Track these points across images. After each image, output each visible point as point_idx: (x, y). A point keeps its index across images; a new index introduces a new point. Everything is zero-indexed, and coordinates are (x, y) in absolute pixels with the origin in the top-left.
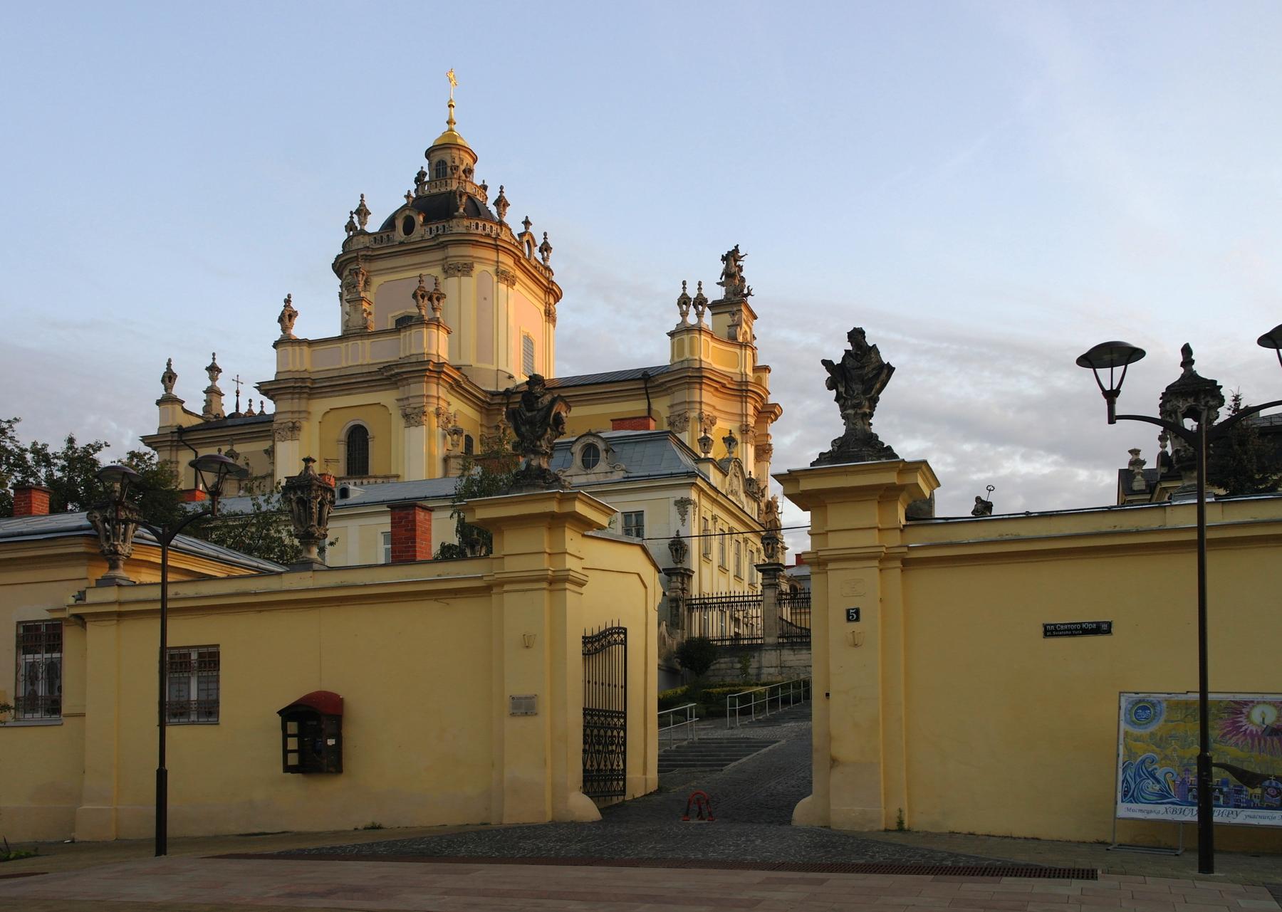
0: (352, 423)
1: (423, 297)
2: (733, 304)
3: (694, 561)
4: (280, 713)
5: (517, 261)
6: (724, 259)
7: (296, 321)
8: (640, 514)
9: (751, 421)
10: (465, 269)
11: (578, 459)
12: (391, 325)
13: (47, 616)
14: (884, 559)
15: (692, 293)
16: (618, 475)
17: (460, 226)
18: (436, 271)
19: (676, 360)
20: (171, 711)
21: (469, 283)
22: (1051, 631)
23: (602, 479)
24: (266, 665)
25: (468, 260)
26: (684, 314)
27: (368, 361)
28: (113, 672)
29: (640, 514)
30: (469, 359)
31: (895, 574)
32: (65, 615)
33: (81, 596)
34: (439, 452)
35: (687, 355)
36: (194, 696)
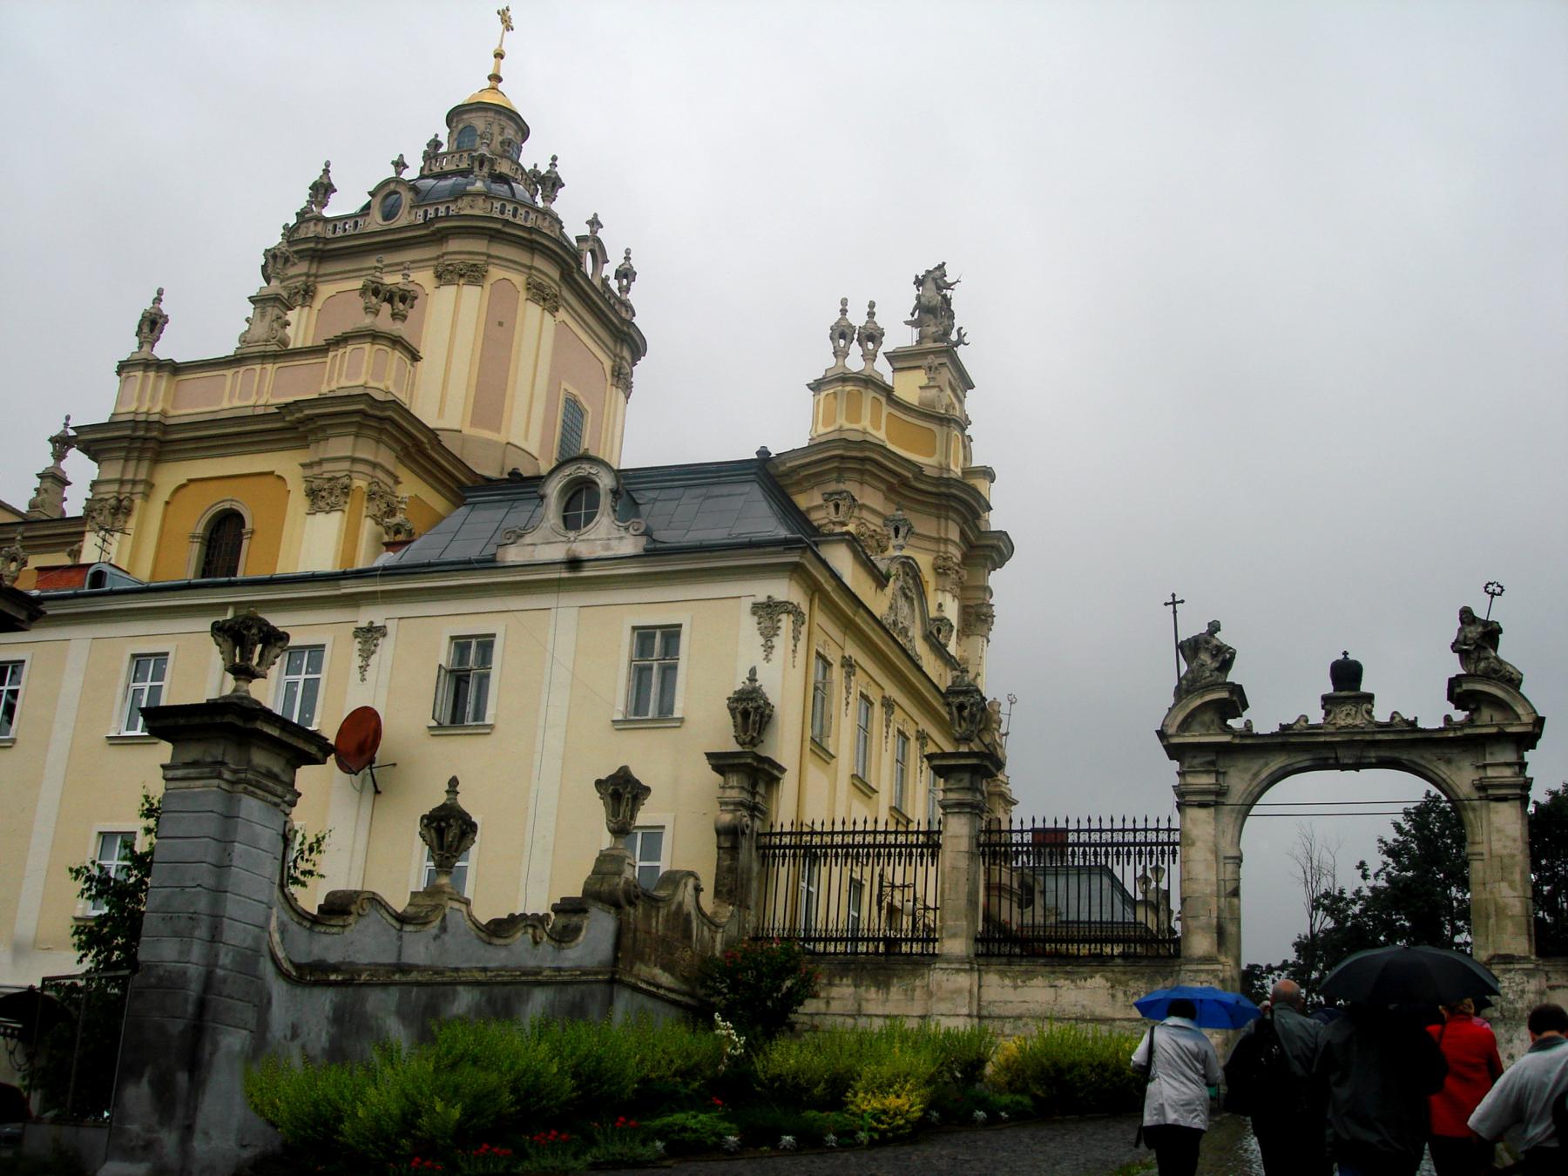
0: (227, 505)
3: (785, 745)
6: (919, 282)
8: (672, 634)
9: (955, 553)
10: (473, 274)
11: (552, 510)
15: (857, 319)
18: (424, 278)
19: (821, 430)
21: (472, 297)
29: (672, 634)
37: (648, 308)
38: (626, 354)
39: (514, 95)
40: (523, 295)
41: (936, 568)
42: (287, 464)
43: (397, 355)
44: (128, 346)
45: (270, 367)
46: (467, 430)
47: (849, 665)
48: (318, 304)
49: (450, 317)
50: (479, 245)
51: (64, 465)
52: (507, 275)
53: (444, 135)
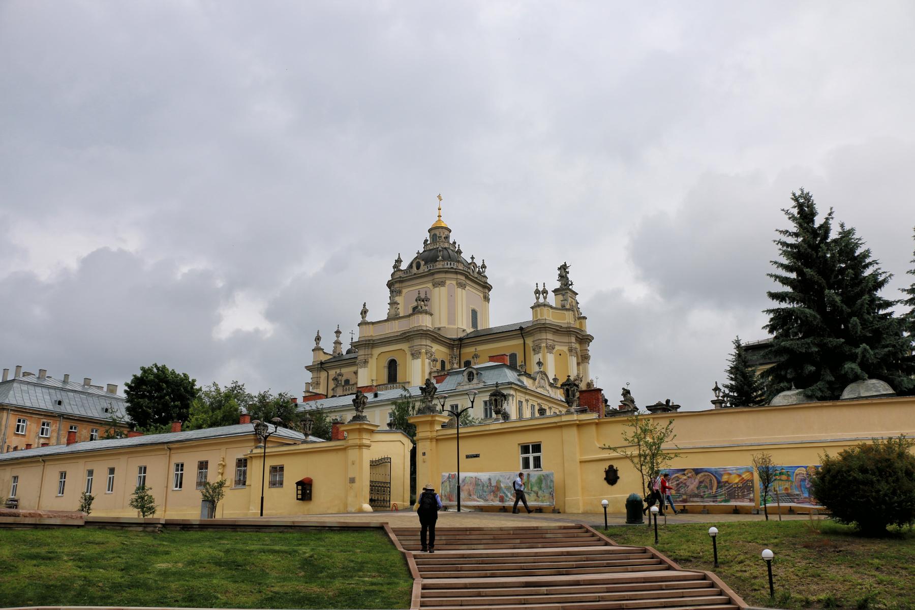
2: (564, 290)
5: (467, 277)
6: (559, 269)
7: (368, 314)
10: (442, 284)
12: (410, 311)
15: (541, 289)
16: (481, 385)
18: (430, 285)
22: (477, 456)
23: (476, 387)
26: (538, 298)
30: (443, 323)
31: (434, 443)
34: (427, 371)
35: (539, 317)
37: (491, 276)
39: (446, 223)
42: (404, 346)
43: (428, 316)
44: (360, 320)
47: (527, 401)
48: (403, 294)
49: (440, 296)
50: (443, 275)
51: (340, 339)
52: (451, 283)
53: (428, 236)
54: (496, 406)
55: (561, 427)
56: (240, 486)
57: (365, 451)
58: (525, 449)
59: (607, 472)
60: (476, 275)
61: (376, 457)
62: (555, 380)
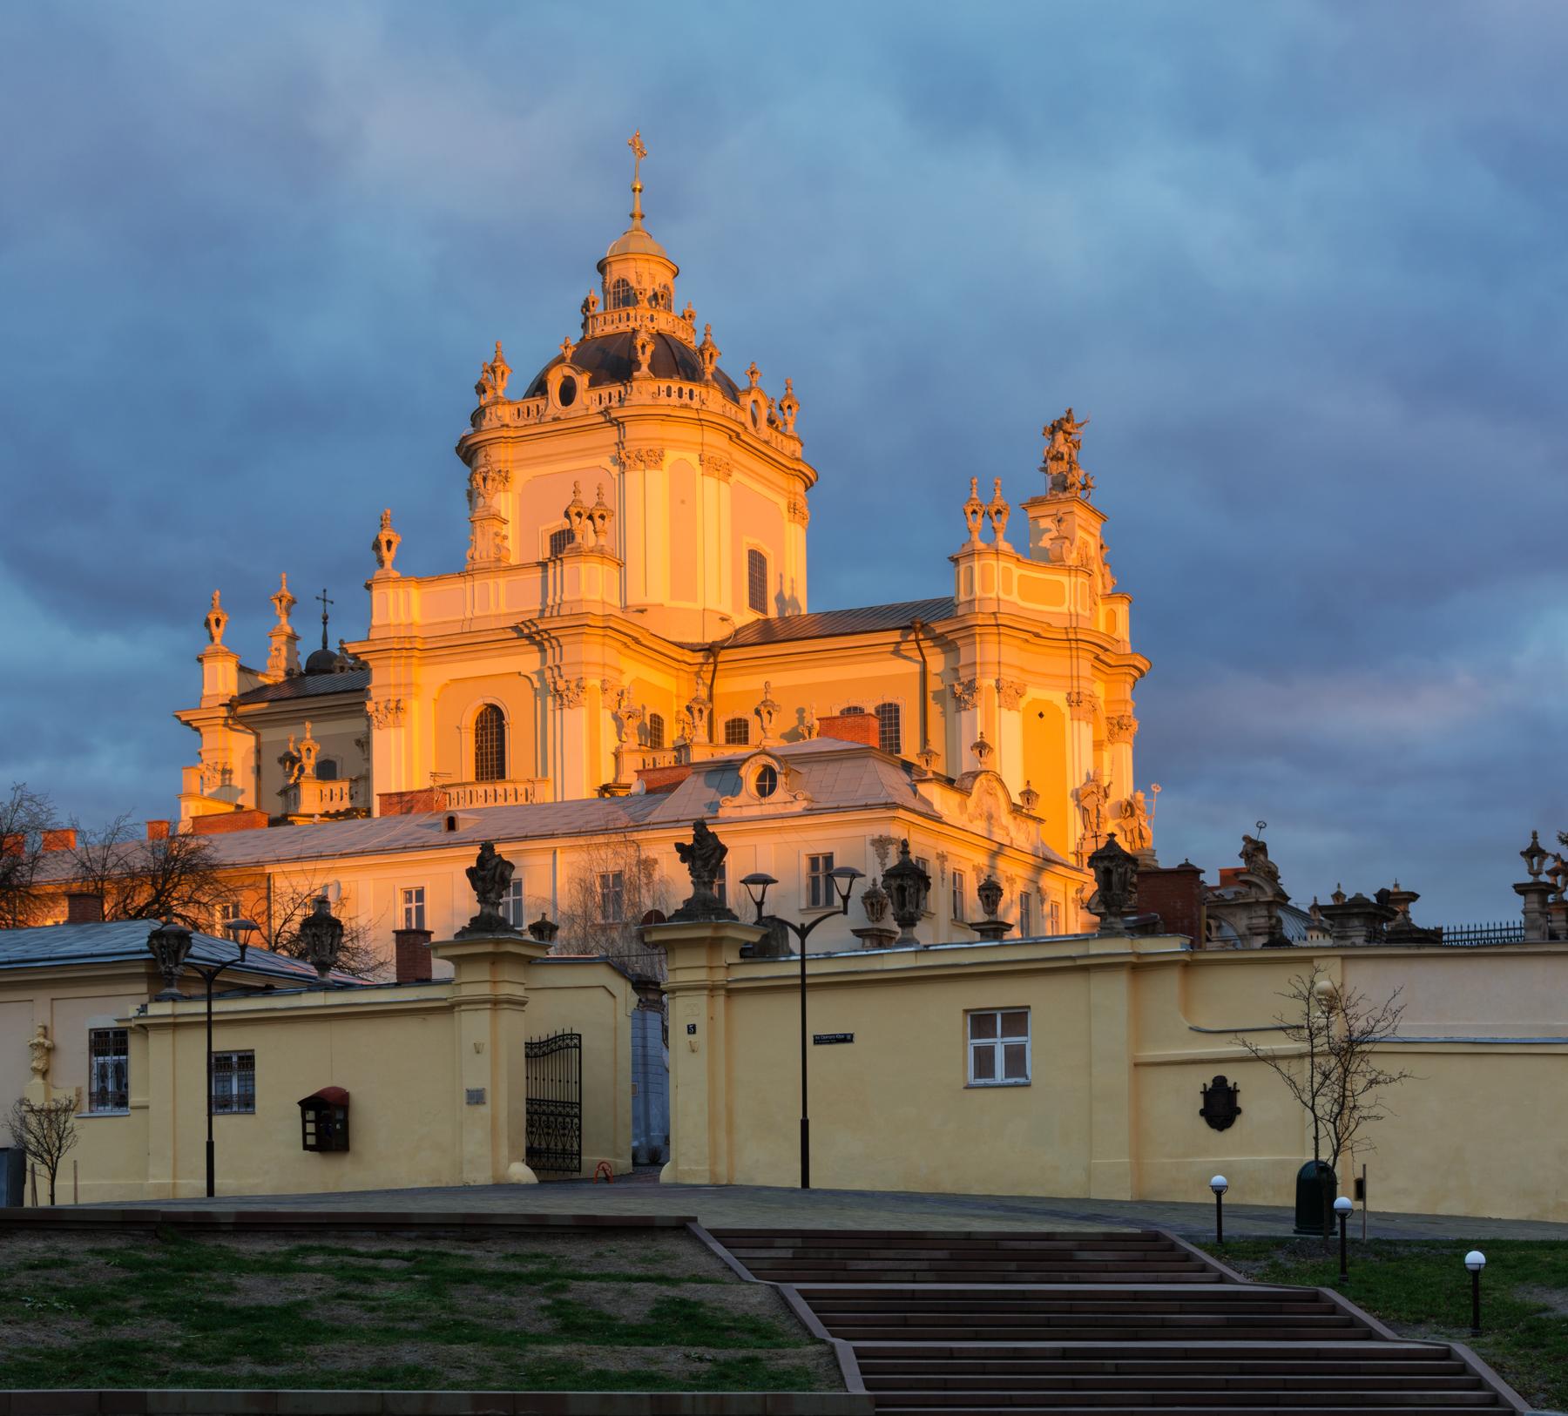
1: (579, 515)
4: (300, 1103)
5: (735, 437)
10: (653, 459)
12: (545, 552)
13: (116, 1025)
14: (712, 989)
17: (646, 389)
20: (218, 1104)
24: (289, 1067)
25: (655, 445)
27: (504, 609)
28: (169, 1071)
31: (720, 1000)
32: (132, 1024)
33: (144, 1008)
36: (235, 1091)
38: (800, 487)
40: (699, 470)
41: (1070, 703)
45: (502, 582)
46: (668, 603)
54: (902, 905)
55: (1085, 969)
56: (108, 1110)
57: (508, 1016)
58: (981, 1022)
59: (1208, 1095)
60: (765, 431)
61: (541, 1033)
62: (1028, 794)
